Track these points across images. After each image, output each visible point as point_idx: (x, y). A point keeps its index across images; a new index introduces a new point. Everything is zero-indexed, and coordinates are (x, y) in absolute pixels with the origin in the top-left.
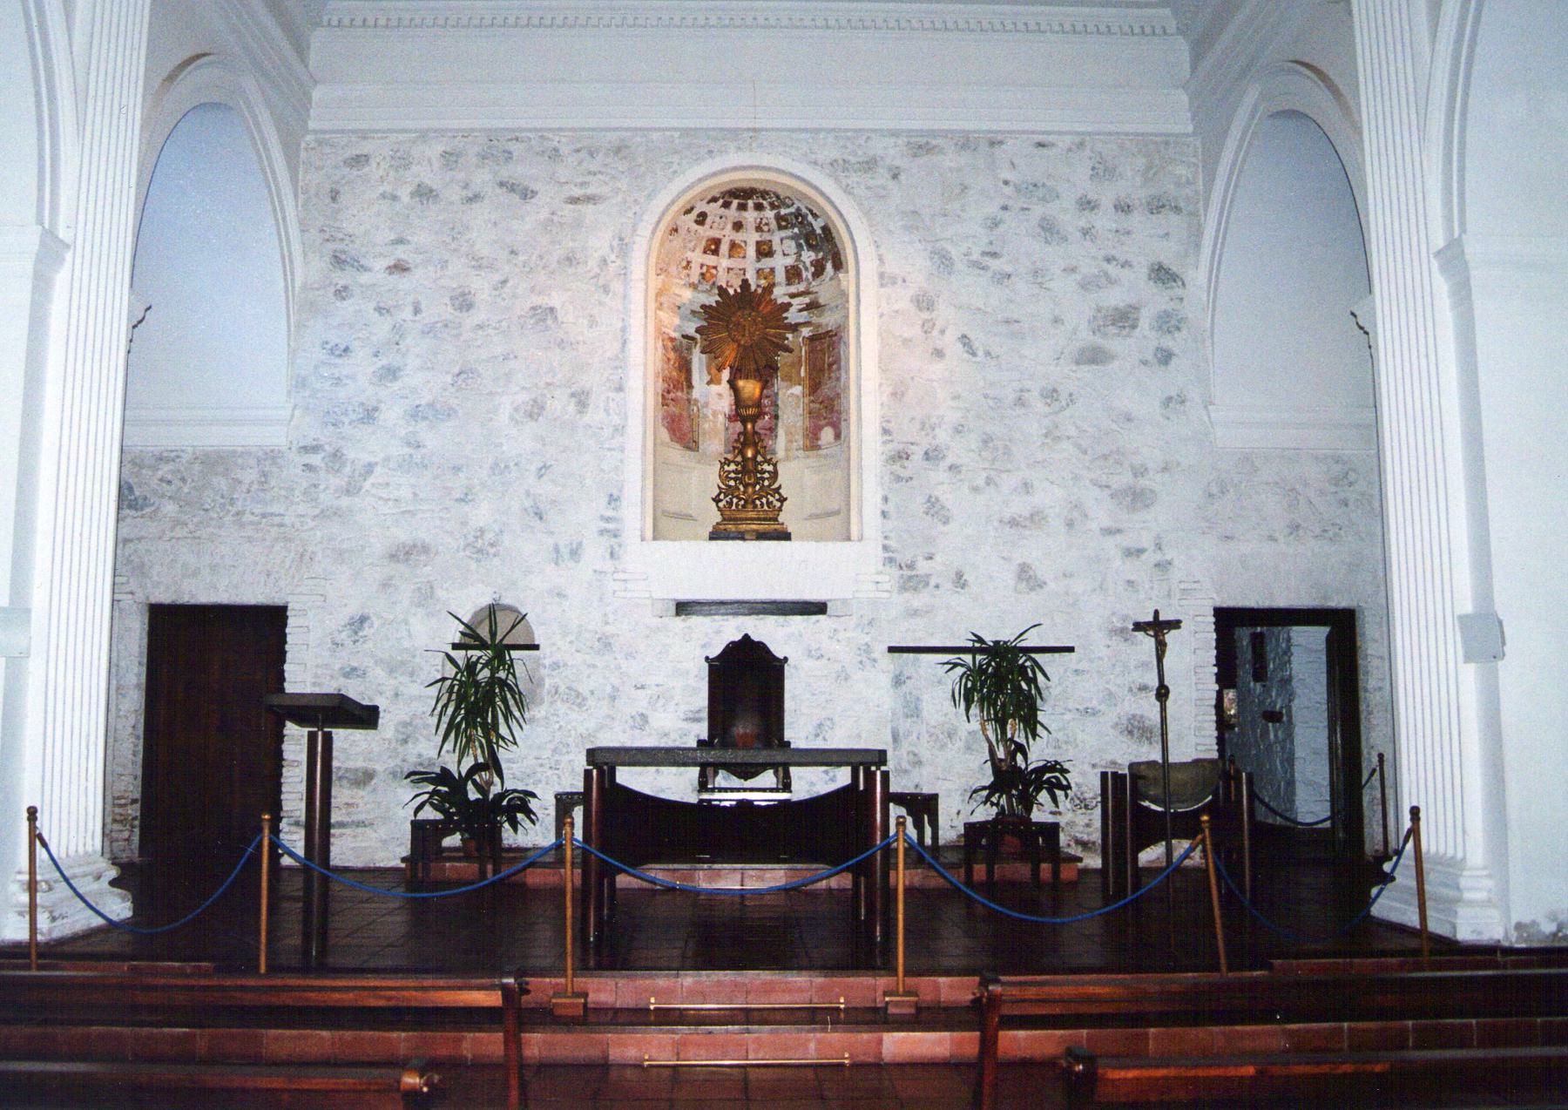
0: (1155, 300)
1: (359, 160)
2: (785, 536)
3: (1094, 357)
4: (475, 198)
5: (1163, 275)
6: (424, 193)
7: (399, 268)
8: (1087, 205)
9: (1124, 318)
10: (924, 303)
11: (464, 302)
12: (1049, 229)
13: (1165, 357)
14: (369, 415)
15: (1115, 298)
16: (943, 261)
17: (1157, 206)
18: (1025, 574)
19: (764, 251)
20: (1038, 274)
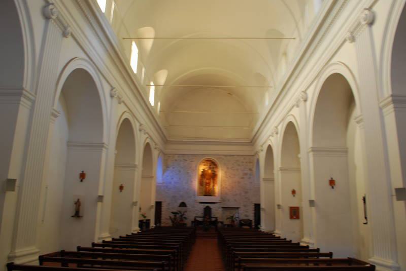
0: (249, 172)
1: (169, 157)
2: (211, 196)
3: (243, 178)
4: (181, 161)
5: (250, 170)
6: (176, 160)
7: (173, 168)
8: (243, 162)
9: (246, 174)
10: (226, 172)
11: (180, 171)
12: (239, 165)
13: (250, 178)
14: (170, 183)
15: (246, 172)
16: (228, 168)
17: (250, 162)
18: (235, 200)
19: (210, 165)
20: (237, 170)
